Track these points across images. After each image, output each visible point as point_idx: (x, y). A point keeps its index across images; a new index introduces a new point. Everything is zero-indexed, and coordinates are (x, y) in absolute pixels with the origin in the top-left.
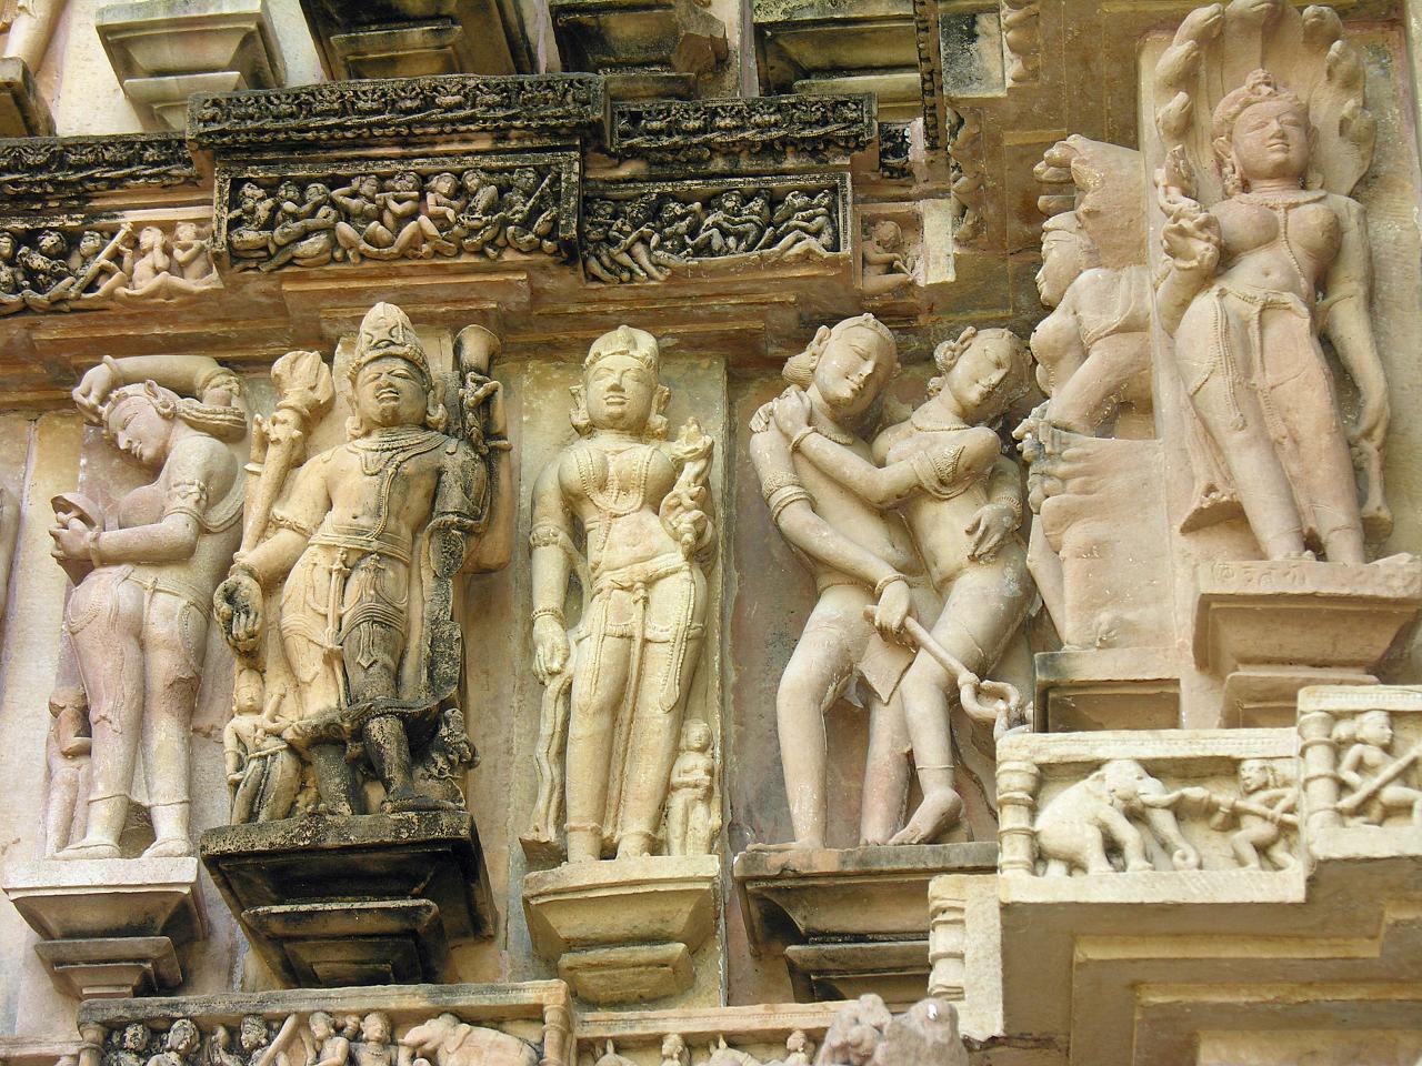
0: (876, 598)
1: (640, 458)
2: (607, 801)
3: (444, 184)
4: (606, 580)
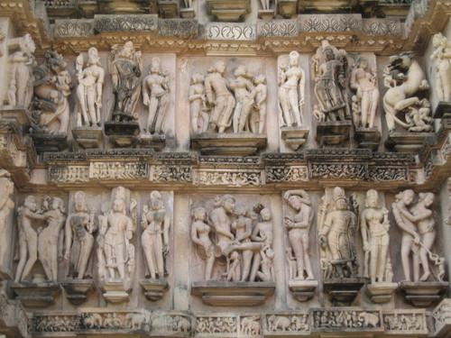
1: (378, 215)
2: (377, 272)
3: (346, 167)
4: (374, 235)
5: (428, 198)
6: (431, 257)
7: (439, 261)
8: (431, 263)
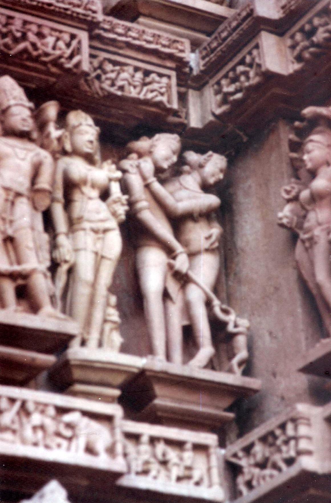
0: (174, 258)
3: (34, 28)
4: (86, 225)
5: (214, 164)
6: (217, 310)
7: (236, 326)
8: (217, 327)
